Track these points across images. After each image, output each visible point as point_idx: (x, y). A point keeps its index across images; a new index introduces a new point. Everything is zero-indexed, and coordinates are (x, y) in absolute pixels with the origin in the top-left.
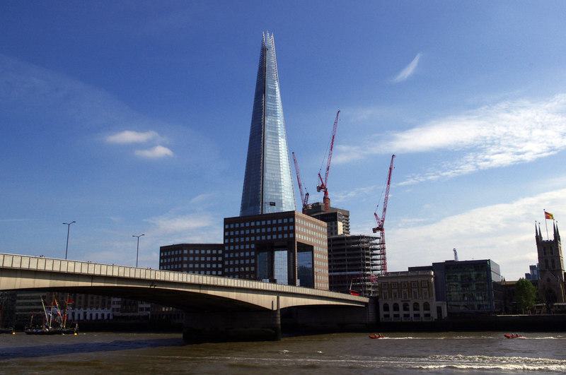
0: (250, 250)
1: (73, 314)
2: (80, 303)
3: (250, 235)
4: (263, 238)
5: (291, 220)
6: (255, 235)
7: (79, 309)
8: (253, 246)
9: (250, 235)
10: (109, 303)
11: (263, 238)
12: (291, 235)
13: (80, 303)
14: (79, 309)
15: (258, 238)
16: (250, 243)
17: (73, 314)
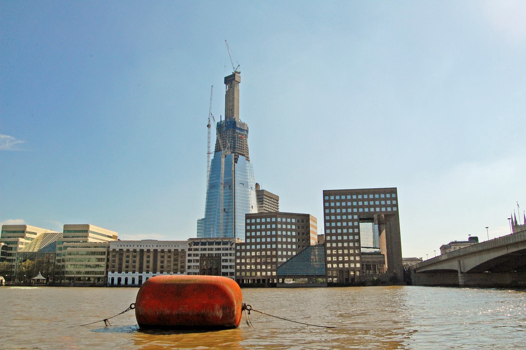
0: (353, 220)
1: (140, 278)
2: (148, 267)
3: (352, 207)
4: (366, 210)
5: (394, 196)
6: (358, 207)
7: (148, 272)
8: (356, 217)
9: (352, 207)
10: (183, 267)
11: (366, 210)
12: (395, 209)
13: (148, 267)
14: (148, 272)
15: (361, 210)
16: (352, 214)
17: (140, 278)
